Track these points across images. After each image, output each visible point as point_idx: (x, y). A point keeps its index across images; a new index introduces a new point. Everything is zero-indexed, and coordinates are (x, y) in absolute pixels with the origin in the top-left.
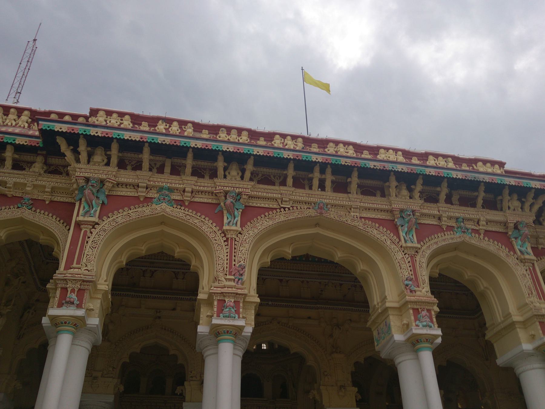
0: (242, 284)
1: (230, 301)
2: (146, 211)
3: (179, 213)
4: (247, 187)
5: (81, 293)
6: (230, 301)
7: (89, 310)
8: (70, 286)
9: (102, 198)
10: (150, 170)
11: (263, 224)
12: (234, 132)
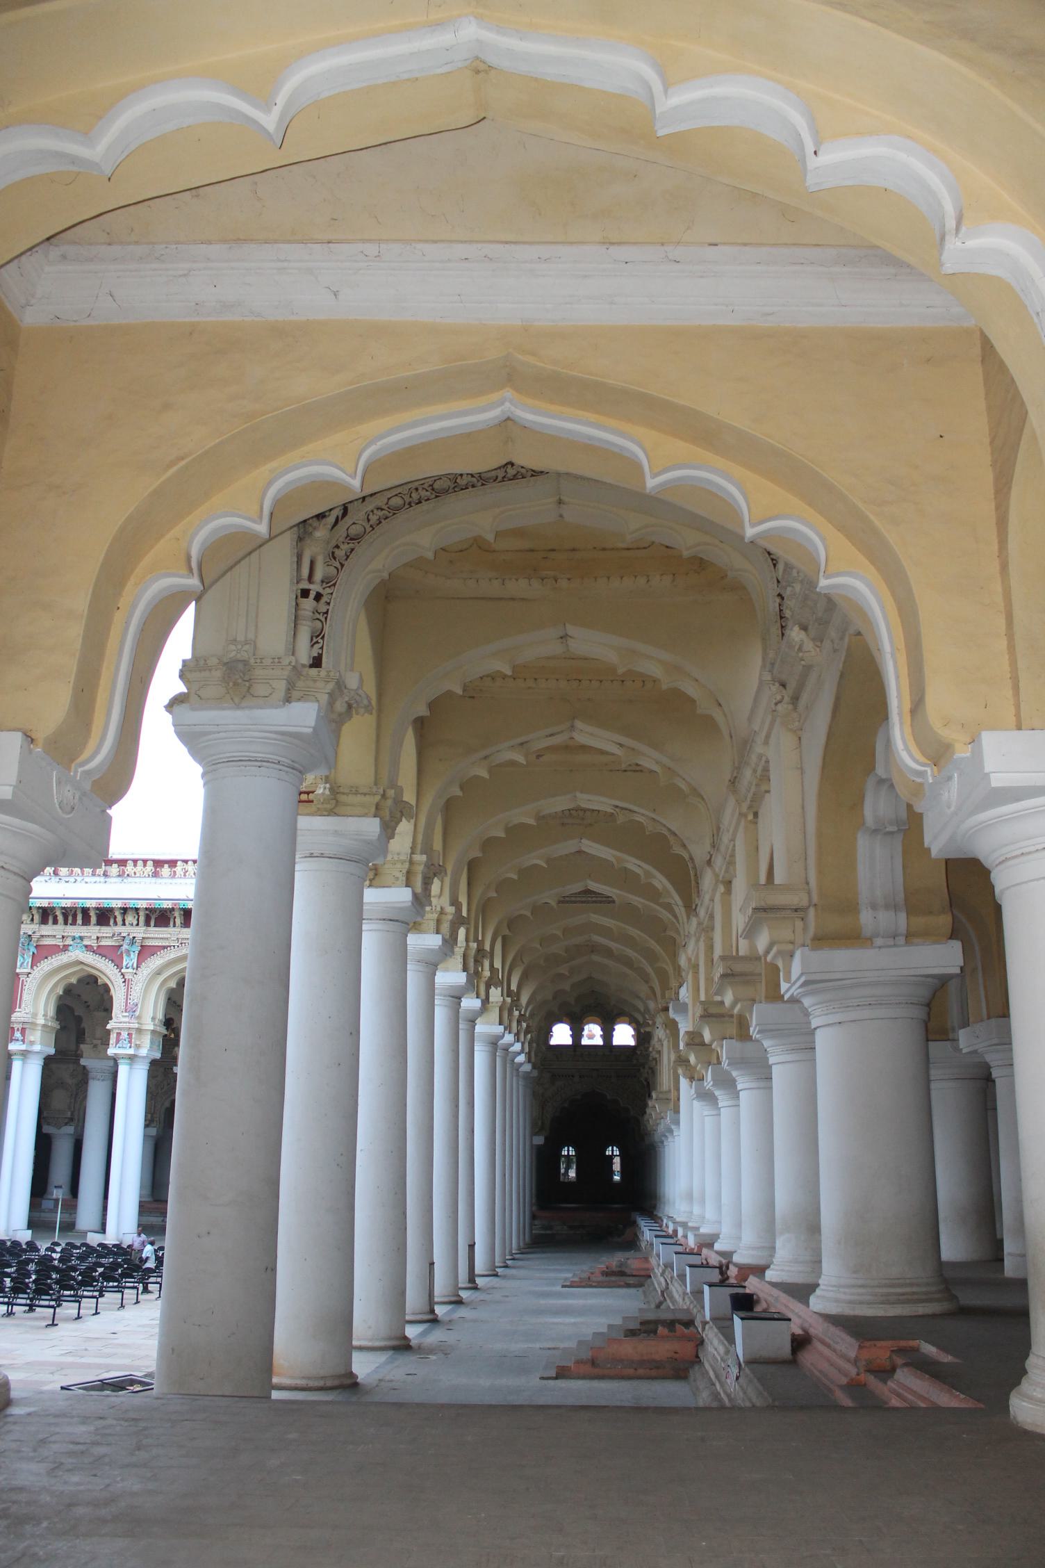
0: (139, 1018)
1: (125, 1035)
2: (63, 958)
3: (90, 958)
4: (140, 932)
5: (23, 1031)
6: (125, 1035)
7: (32, 1043)
8: (16, 1026)
9: (33, 949)
10: (66, 923)
11: (155, 962)
12: (140, 863)
